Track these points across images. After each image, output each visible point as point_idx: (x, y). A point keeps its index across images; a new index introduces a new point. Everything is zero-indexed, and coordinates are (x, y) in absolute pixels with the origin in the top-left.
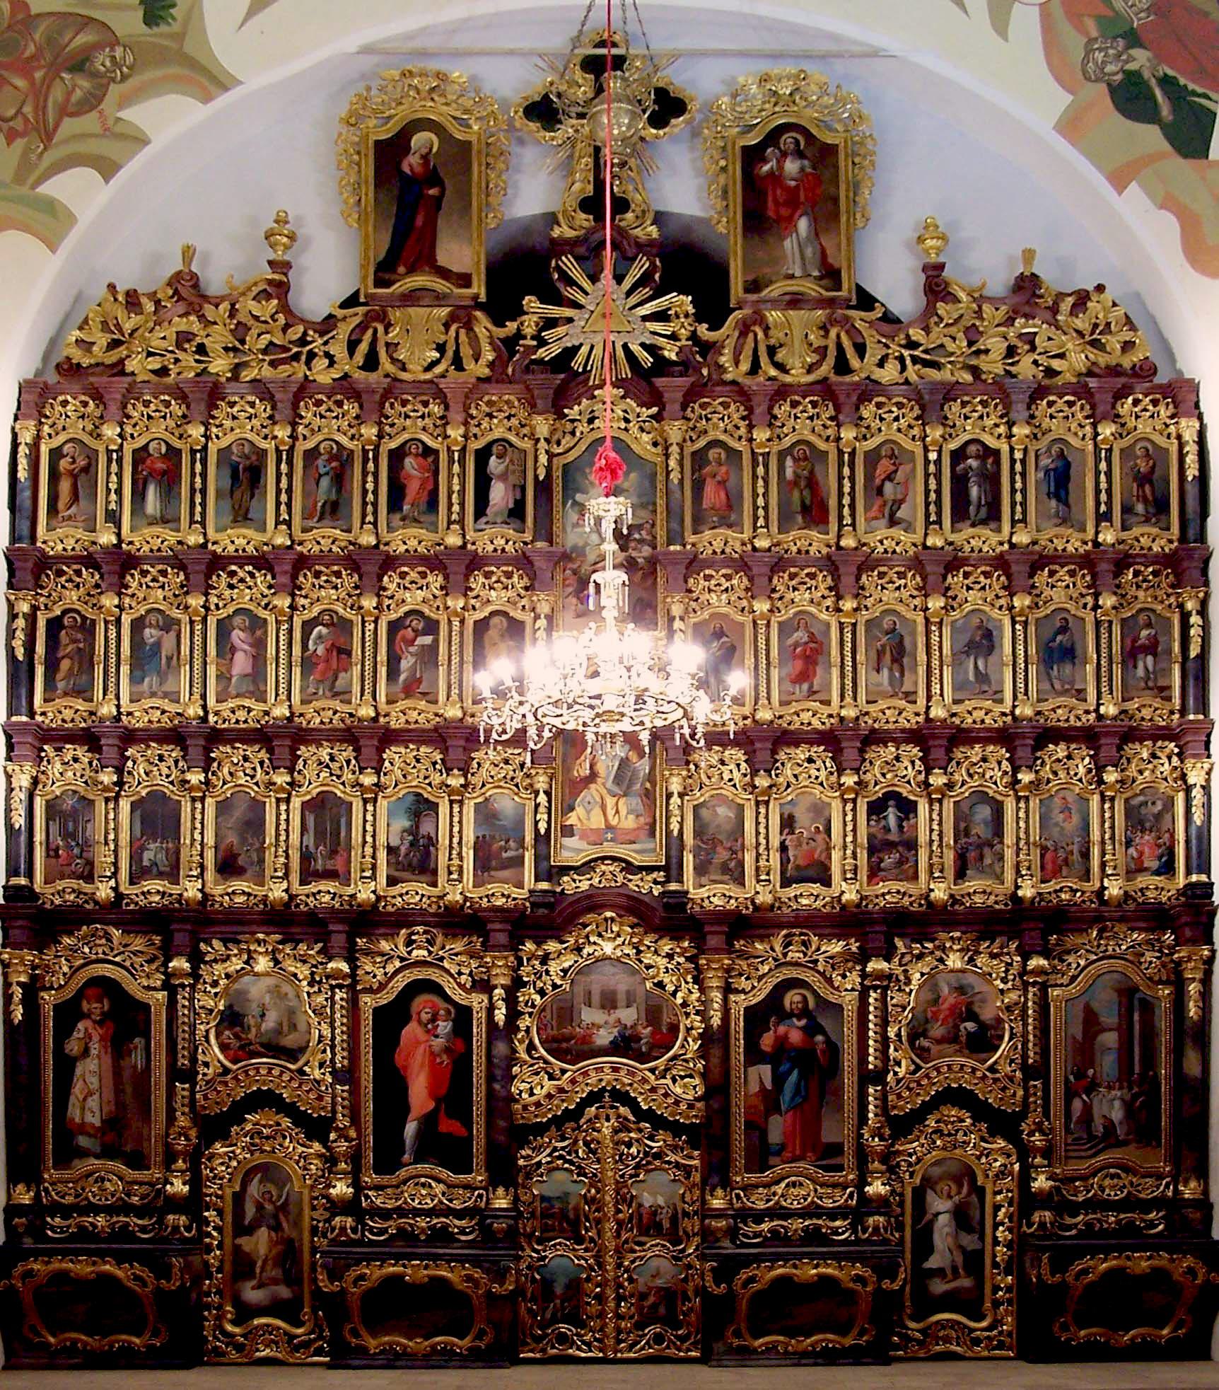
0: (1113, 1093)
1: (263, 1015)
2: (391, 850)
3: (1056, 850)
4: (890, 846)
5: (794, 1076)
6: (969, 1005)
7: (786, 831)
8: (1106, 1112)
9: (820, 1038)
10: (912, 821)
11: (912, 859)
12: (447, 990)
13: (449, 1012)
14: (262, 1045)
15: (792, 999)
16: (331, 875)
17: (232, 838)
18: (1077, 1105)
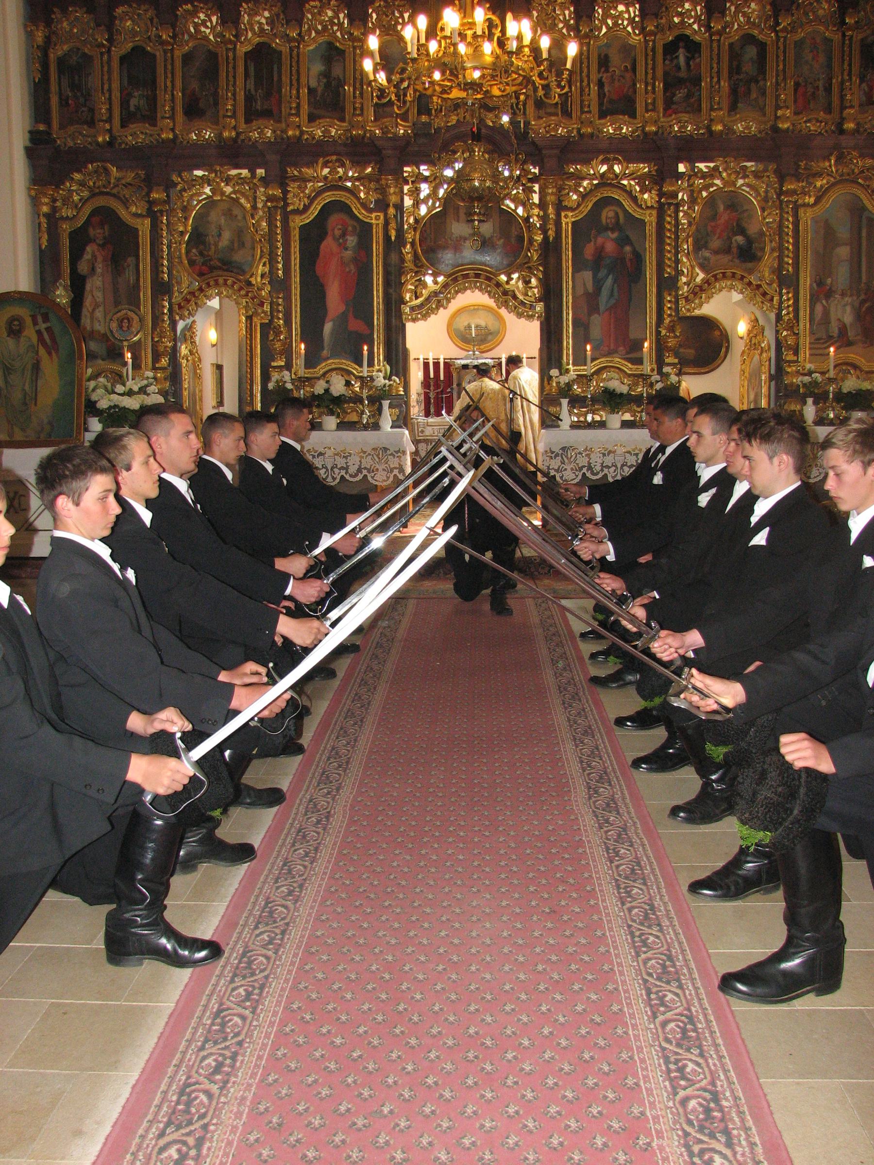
0: (846, 299)
1: (220, 235)
2: (311, 91)
3: (806, 86)
4: (681, 82)
5: (609, 281)
6: (739, 221)
7: (603, 70)
8: (840, 317)
9: (628, 249)
10: (698, 60)
11: (697, 94)
12: (354, 210)
13: (354, 227)
14: (219, 260)
15: (607, 214)
16: (267, 114)
17: (195, 85)
18: (819, 308)
